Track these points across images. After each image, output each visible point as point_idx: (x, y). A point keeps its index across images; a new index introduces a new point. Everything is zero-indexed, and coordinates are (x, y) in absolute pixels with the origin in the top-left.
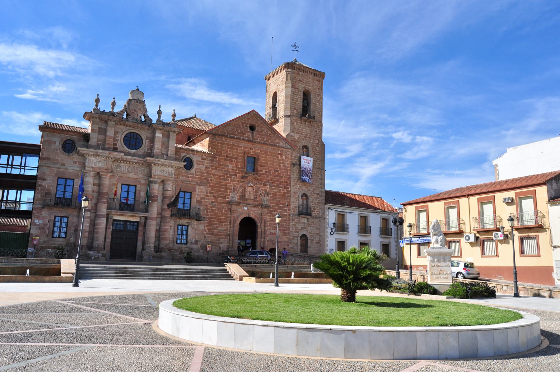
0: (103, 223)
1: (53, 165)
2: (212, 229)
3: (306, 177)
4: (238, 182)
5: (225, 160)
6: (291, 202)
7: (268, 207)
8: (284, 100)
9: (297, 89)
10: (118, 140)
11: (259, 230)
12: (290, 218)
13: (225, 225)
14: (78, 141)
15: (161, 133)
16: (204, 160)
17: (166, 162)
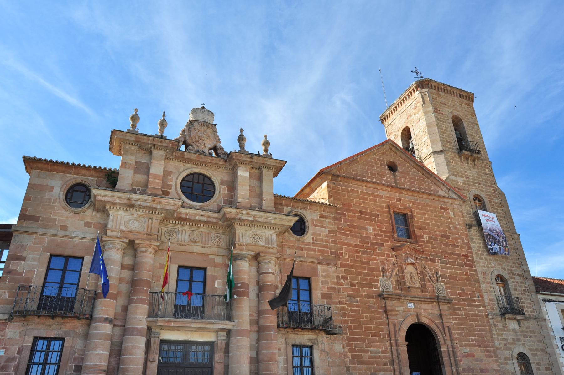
0: (139, 347)
1: (43, 230)
2: (359, 351)
3: (496, 245)
4: (388, 255)
5: (359, 218)
6: (483, 291)
7: (449, 301)
8: (427, 131)
9: (442, 114)
10: (171, 185)
11: (443, 349)
12: (488, 321)
13: (381, 341)
14: (97, 185)
15: (247, 171)
16: (324, 219)
17: (260, 216)
